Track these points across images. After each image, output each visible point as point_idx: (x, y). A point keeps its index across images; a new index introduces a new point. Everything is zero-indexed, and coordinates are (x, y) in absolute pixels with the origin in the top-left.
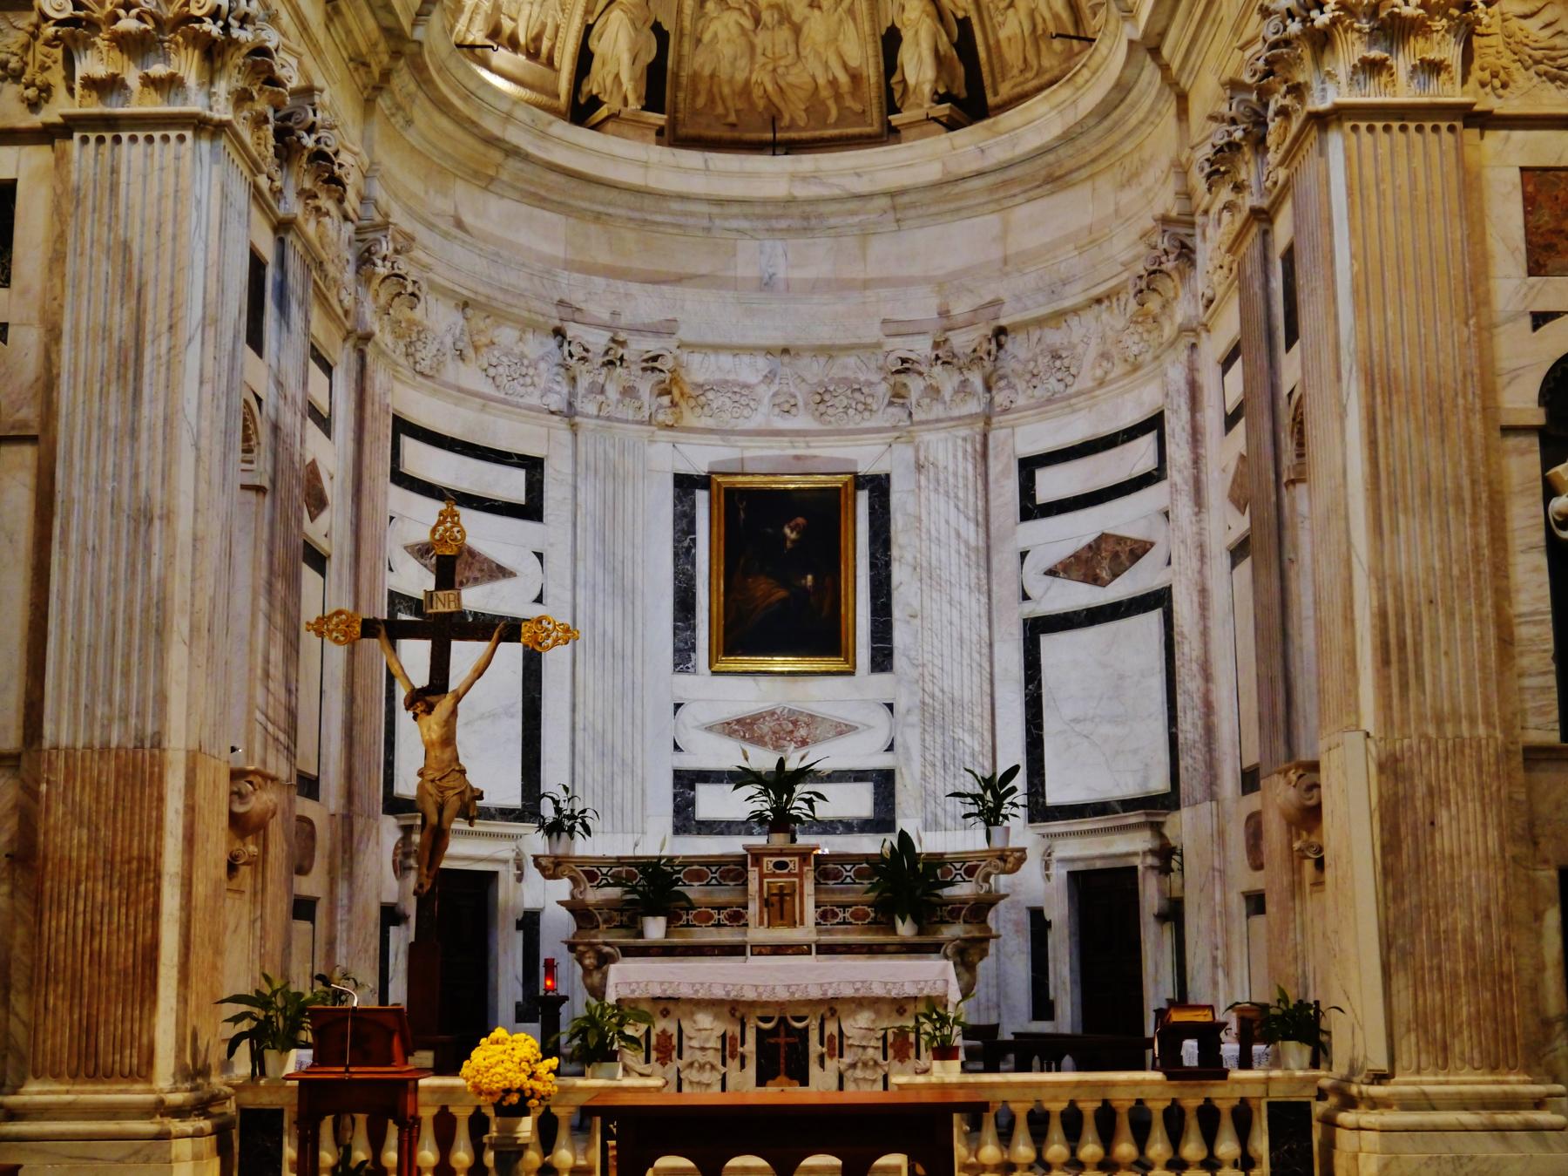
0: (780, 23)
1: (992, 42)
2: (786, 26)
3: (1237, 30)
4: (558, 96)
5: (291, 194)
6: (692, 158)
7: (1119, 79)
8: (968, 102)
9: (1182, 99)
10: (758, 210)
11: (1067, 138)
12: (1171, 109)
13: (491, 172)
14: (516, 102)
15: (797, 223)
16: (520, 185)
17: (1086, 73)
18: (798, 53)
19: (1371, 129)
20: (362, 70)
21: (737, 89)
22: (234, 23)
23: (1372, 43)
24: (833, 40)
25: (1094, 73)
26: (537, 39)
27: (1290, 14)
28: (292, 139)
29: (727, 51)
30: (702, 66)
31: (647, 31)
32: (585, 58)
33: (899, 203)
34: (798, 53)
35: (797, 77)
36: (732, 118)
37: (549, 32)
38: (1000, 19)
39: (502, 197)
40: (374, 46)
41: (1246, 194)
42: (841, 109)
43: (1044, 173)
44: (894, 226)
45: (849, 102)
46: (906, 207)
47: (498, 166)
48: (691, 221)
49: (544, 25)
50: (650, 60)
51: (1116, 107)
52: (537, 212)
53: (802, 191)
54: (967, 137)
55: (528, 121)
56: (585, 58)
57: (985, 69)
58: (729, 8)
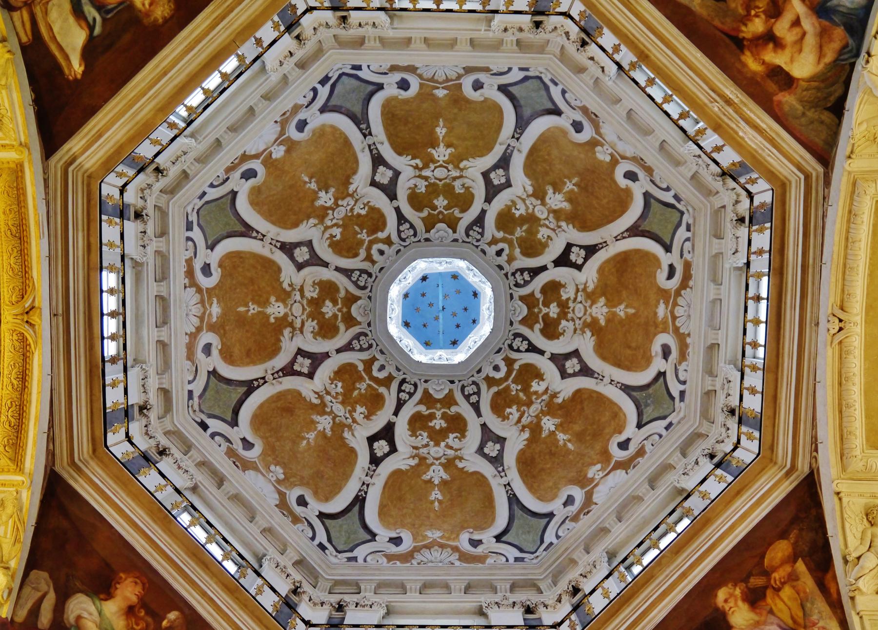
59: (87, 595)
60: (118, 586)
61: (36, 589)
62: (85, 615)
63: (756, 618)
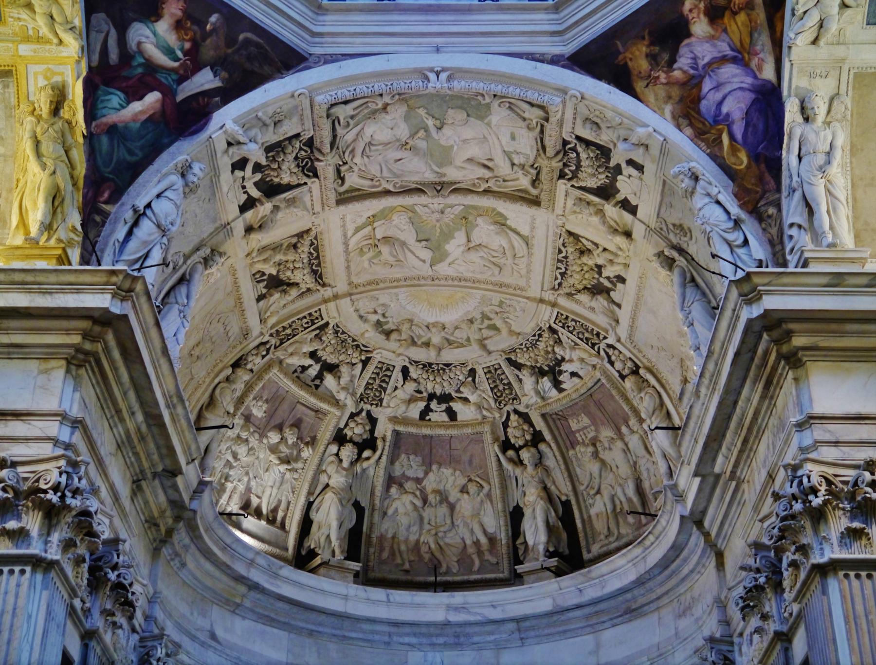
0: (441, 502)
1: (585, 517)
2: (445, 504)
3: (756, 509)
4: (287, 550)
5: (96, 613)
6: (378, 593)
7: (675, 541)
8: (570, 556)
9: (720, 556)
10: (424, 630)
11: (640, 582)
12: (712, 563)
13: (238, 600)
14: (258, 553)
15: (451, 640)
16: (258, 610)
17: (651, 538)
18: (453, 523)
19: (858, 576)
20: (153, 529)
21: (410, 547)
22: (69, 494)
23: (852, 519)
24: (476, 514)
25: (657, 538)
26: (275, 510)
27: (794, 497)
28: (102, 573)
29: (404, 521)
30: (387, 531)
31: (350, 507)
32: (306, 524)
33: (524, 627)
34: (453, 523)
35: (452, 539)
36: (407, 566)
37: (283, 506)
38: (591, 501)
39: (244, 618)
40: (163, 512)
41: (770, 621)
42: (482, 561)
43: (624, 606)
44: (519, 643)
45: (487, 556)
46: (527, 629)
47: (244, 596)
48: (377, 637)
49: (280, 502)
50: (350, 526)
51: (673, 562)
52: (268, 629)
53: (454, 618)
54: (567, 581)
55: (266, 566)
56: (306, 524)
57: (581, 535)
58: (406, 492)
59: (141, 22)
60: (164, 6)
61: (99, 31)
62: (144, 40)
63: (712, 32)
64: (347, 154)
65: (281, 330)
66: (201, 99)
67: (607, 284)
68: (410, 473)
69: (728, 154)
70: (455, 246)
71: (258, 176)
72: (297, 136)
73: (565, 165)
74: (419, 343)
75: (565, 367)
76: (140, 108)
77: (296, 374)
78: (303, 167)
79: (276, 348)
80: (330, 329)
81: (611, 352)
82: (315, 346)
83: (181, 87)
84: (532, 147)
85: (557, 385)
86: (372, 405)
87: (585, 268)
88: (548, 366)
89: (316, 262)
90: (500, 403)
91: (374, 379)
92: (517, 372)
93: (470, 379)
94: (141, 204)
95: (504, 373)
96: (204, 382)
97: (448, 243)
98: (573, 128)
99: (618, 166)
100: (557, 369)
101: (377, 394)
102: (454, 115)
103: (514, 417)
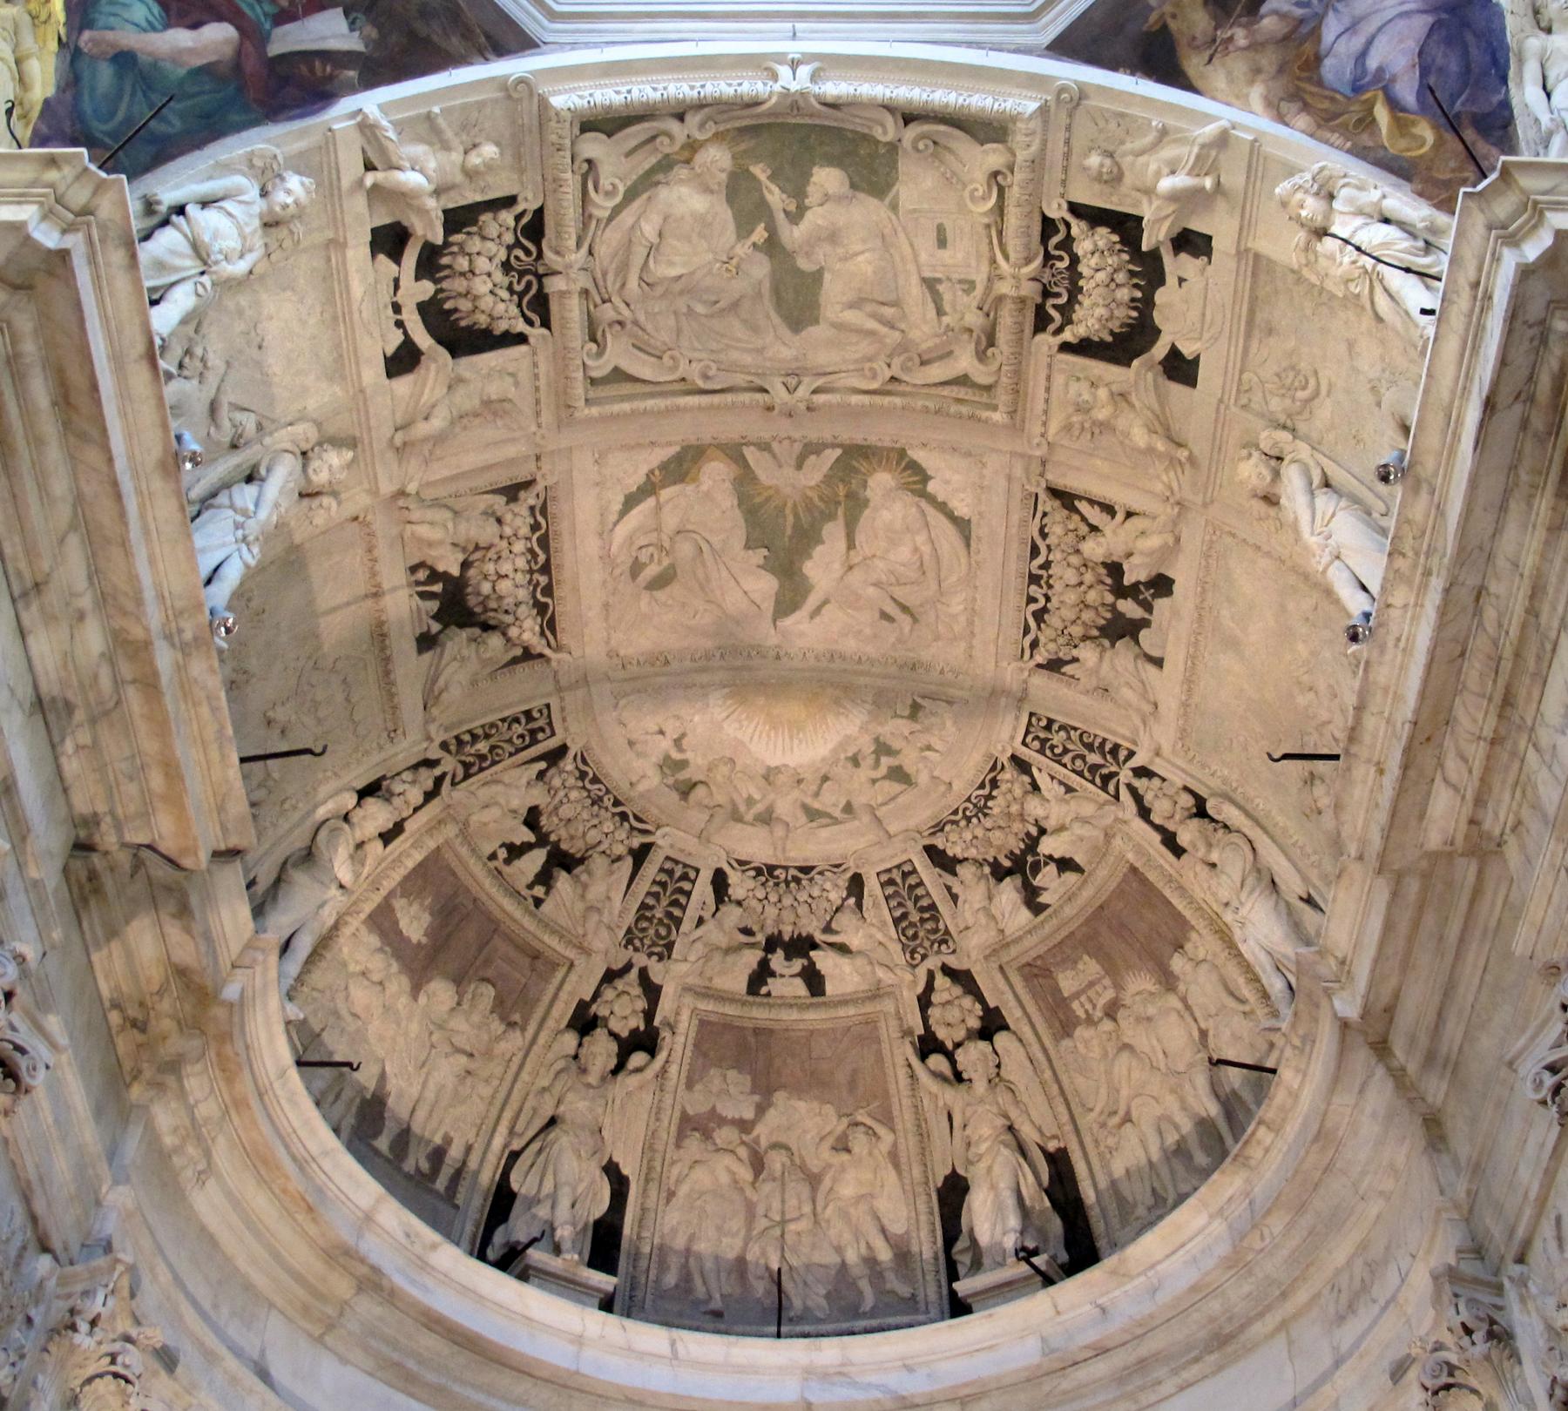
8: (1074, 1237)
36: (717, 1304)
38: (1111, 1141)
42: (880, 1291)
54: (1072, 1290)
58: (718, 1150)
64: (610, 277)
65: (467, 738)
66: (317, 64)
67: (1129, 608)
68: (729, 1111)
69: (1390, 130)
70: (822, 567)
71: (427, 289)
72: (510, 201)
73: (1046, 293)
74: (749, 817)
75: (1047, 846)
76: (190, 44)
77: (492, 864)
78: (521, 295)
79: (453, 784)
80: (568, 764)
81: (1141, 784)
82: (538, 796)
83: (279, 31)
84: (979, 257)
85: (1032, 899)
86: (650, 955)
87: (1089, 577)
88: (1011, 855)
89: (543, 580)
90: (913, 952)
91: (656, 896)
92: (949, 879)
93: (852, 901)
94: (168, 197)
95: (921, 884)
96: (295, 808)
97: (810, 557)
98: (1064, 182)
99: (1155, 255)
100: (1030, 859)
101: (663, 932)
102: (827, 179)
103: (941, 981)
